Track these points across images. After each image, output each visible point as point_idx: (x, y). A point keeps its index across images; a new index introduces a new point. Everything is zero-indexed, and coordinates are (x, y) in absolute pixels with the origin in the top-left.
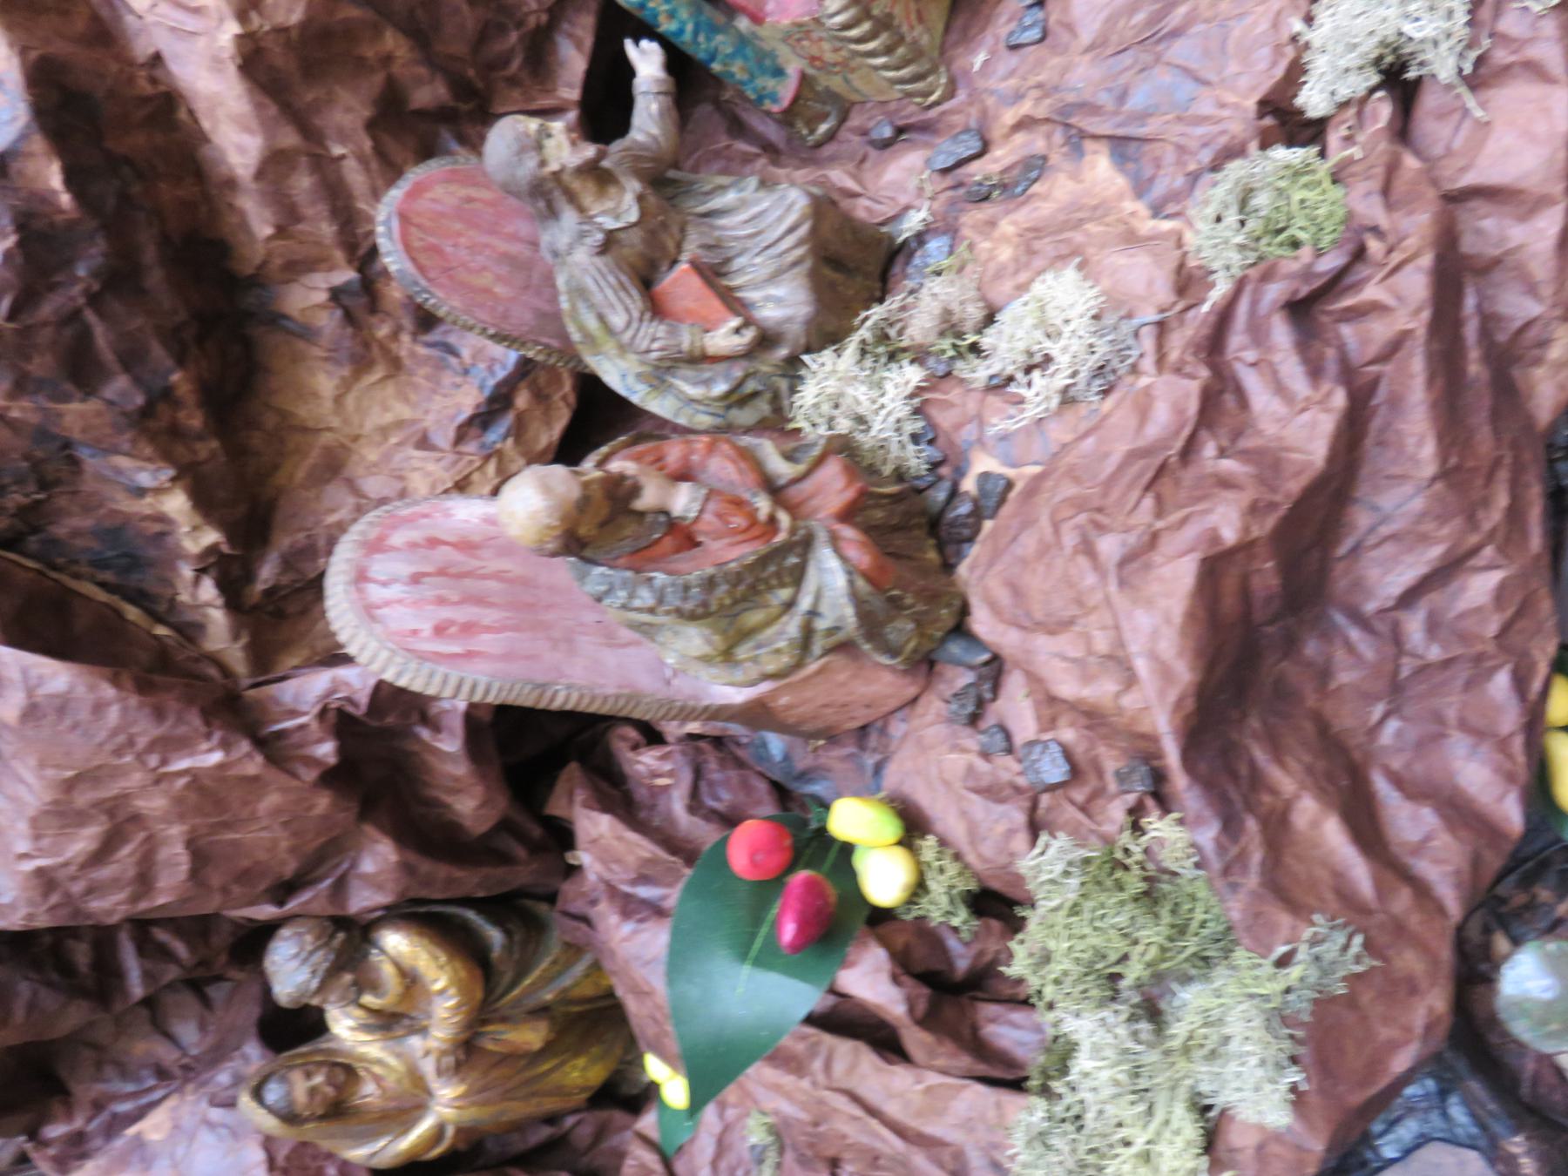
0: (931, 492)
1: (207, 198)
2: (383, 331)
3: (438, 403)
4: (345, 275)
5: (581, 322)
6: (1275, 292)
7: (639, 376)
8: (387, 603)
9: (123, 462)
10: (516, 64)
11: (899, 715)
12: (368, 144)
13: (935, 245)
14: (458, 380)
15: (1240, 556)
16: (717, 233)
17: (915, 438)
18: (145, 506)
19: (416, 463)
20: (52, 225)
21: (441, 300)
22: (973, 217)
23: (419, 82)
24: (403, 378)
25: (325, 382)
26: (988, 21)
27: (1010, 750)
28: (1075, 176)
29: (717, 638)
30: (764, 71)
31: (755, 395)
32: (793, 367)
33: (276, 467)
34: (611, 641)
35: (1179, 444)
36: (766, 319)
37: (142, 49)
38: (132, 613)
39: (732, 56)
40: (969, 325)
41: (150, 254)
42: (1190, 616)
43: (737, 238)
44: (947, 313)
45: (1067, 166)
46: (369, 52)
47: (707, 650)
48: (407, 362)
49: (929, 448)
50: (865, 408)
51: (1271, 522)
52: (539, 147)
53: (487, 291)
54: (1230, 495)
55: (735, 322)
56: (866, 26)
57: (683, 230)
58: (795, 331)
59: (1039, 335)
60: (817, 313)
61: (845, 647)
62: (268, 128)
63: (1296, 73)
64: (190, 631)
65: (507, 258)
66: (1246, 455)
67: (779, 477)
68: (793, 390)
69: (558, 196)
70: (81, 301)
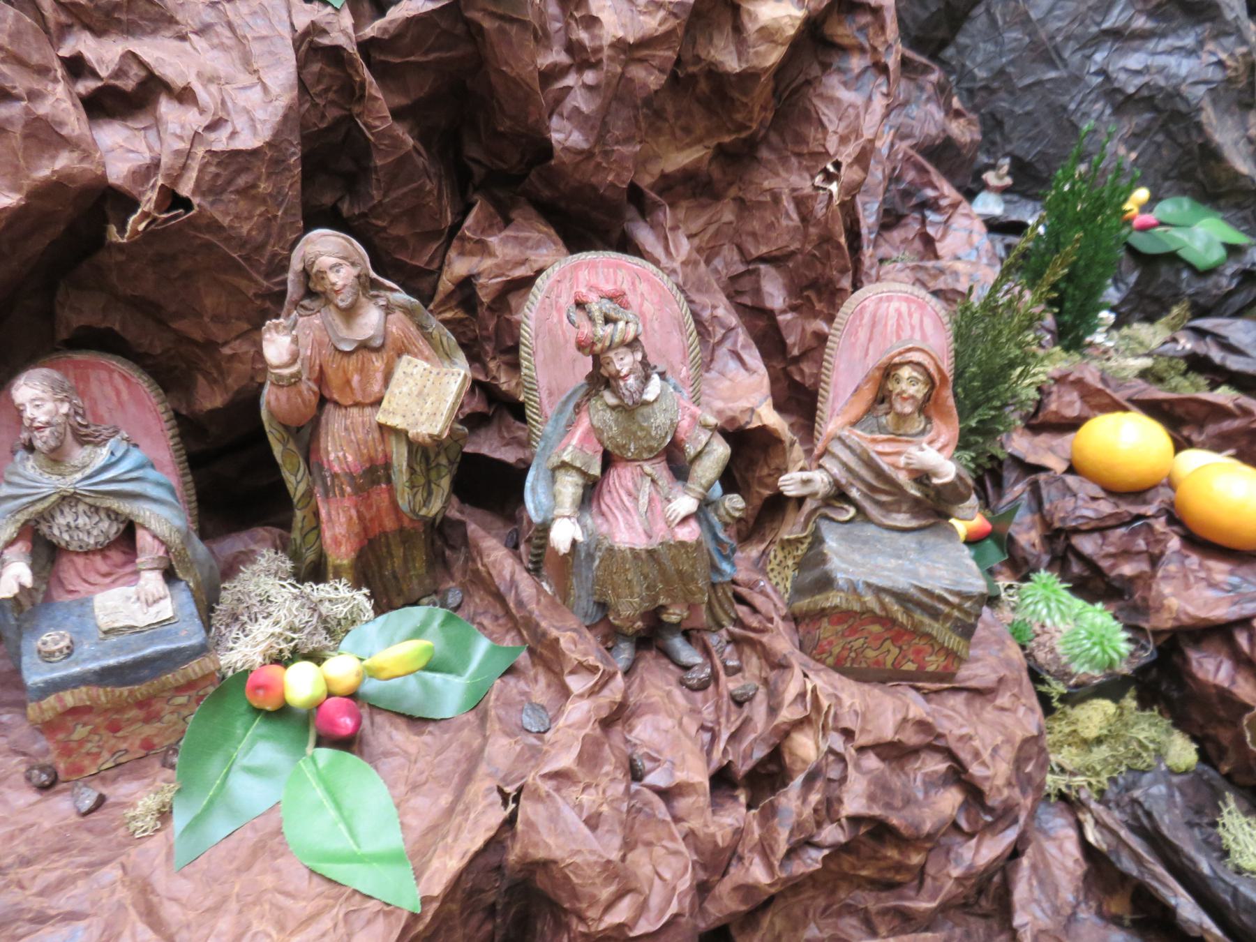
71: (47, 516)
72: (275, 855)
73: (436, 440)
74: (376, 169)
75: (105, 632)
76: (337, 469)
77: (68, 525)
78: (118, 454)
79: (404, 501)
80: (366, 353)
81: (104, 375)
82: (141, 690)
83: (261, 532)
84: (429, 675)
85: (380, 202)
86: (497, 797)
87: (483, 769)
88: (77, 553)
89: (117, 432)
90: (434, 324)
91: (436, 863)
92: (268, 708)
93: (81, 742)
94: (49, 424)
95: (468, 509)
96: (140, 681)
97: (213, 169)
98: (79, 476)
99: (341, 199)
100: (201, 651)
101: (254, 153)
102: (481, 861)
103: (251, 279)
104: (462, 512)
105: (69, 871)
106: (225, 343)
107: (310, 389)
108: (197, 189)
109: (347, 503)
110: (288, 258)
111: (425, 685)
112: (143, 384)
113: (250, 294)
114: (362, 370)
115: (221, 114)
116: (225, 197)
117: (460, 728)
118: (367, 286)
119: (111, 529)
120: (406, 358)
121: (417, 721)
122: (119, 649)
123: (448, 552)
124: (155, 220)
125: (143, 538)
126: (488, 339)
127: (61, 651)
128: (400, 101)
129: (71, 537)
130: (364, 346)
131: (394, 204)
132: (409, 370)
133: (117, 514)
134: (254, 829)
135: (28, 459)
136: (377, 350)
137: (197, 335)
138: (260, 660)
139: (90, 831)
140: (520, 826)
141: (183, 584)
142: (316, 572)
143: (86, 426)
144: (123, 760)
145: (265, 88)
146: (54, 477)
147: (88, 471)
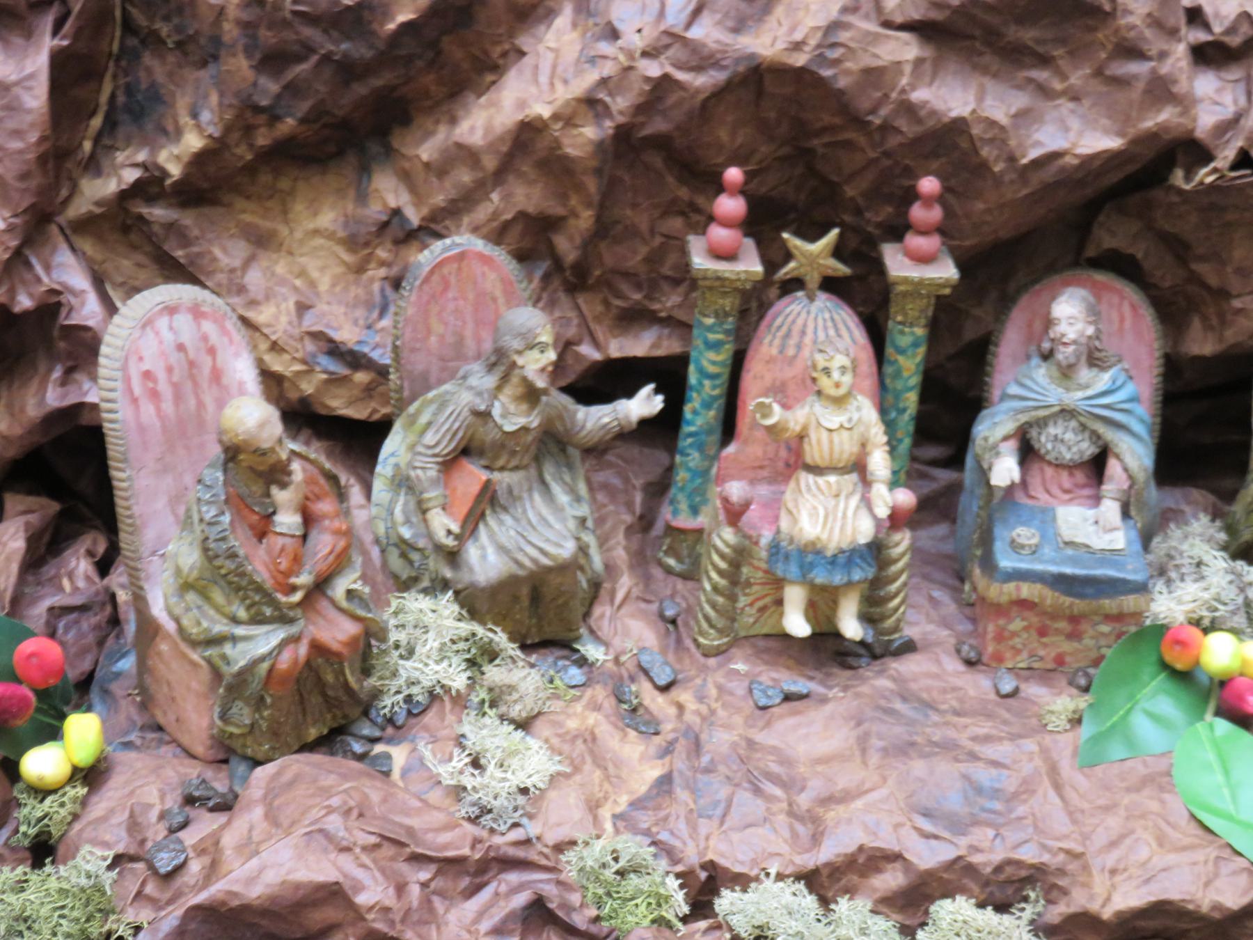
0: (368, 723)
1: (438, 104)
2: (382, 253)
3: (340, 310)
4: (414, 216)
5: (423, 410)
6: (550, 890)
7: (397, 466)
8: (157, 333)
9: (214, 98)
11: (178, 750)
12: (508, 216)
13: (576, 674)
14: (361, 322)
15: (352, 914)
16: (525, 495)
17: (408, 699)
18: (185, 120)
19: (283, 306)
20: (370, 22)
21: (409, 300)
22: (600, 693)
23: (571, 239)
24: (351, 277)
25: (328, 218)
26: (772, 664)
27: (172, 831)
28: (642, 758)
29: (195, 574)
30: (690, 497)
31: (411, 562)
33: (248, 198)
34: (175, 500)
35: (420, 850)
36: (467, 552)
37: (524, 41)
38: (97, 122)
39: (689, 469)
40: (503, 709)
41: (377, 82)
42: (298, 886)
43: (525, 511)
44: (511, 688)
45: (652, 750)
46: (574, 201)
47: (186, 569)
48: (365, 277)
49: (404, 713)
50: (420, 650)
51: (380, 926)
52: (531, 347)
53: (429, 332)
54: (391, 891)
55: (455, 528)
56: (723, 565)
57: (516, 468)
58: (464, 578)
59: (499, 754)
60: (483, 590)
61: (217, 675)
62: (491, 147)
63: (742, 881)
64: (93, 166)
65: (460, 342)
66: (427, 903)
67: (333, 589)
68: (425, 591)
69: (501, 369)
70: (323, 52)
71: (1042, 423)
72: (1162, 789)
75: (1066, 543)
77: (1056, 436)
78: (1119, 383)
81: (1116, 299)
82: (1079, 605)
83: (1196, 494)
88: (1050, 463)
89: (1120, 361)
92: (1179, 666)
93: (1014, 634)
94: (1075, 342)
98: (1080, 394)
105: (994, 732)
106: (1239, 296)
112: (1148, 315)
119: (1088, 449)
122: (1074, 561)
125: (1113, 467)
127: (1030, 546)
129: (1054, 448)
133: (1099, 437)
134: (1145, 764)
135: (1039, 366)
137: (1213, 281)
138: (1181, 618)
139: (1008, 710)
144: (1036, 665)
146: (1060, 390)
147: (1090, 392)
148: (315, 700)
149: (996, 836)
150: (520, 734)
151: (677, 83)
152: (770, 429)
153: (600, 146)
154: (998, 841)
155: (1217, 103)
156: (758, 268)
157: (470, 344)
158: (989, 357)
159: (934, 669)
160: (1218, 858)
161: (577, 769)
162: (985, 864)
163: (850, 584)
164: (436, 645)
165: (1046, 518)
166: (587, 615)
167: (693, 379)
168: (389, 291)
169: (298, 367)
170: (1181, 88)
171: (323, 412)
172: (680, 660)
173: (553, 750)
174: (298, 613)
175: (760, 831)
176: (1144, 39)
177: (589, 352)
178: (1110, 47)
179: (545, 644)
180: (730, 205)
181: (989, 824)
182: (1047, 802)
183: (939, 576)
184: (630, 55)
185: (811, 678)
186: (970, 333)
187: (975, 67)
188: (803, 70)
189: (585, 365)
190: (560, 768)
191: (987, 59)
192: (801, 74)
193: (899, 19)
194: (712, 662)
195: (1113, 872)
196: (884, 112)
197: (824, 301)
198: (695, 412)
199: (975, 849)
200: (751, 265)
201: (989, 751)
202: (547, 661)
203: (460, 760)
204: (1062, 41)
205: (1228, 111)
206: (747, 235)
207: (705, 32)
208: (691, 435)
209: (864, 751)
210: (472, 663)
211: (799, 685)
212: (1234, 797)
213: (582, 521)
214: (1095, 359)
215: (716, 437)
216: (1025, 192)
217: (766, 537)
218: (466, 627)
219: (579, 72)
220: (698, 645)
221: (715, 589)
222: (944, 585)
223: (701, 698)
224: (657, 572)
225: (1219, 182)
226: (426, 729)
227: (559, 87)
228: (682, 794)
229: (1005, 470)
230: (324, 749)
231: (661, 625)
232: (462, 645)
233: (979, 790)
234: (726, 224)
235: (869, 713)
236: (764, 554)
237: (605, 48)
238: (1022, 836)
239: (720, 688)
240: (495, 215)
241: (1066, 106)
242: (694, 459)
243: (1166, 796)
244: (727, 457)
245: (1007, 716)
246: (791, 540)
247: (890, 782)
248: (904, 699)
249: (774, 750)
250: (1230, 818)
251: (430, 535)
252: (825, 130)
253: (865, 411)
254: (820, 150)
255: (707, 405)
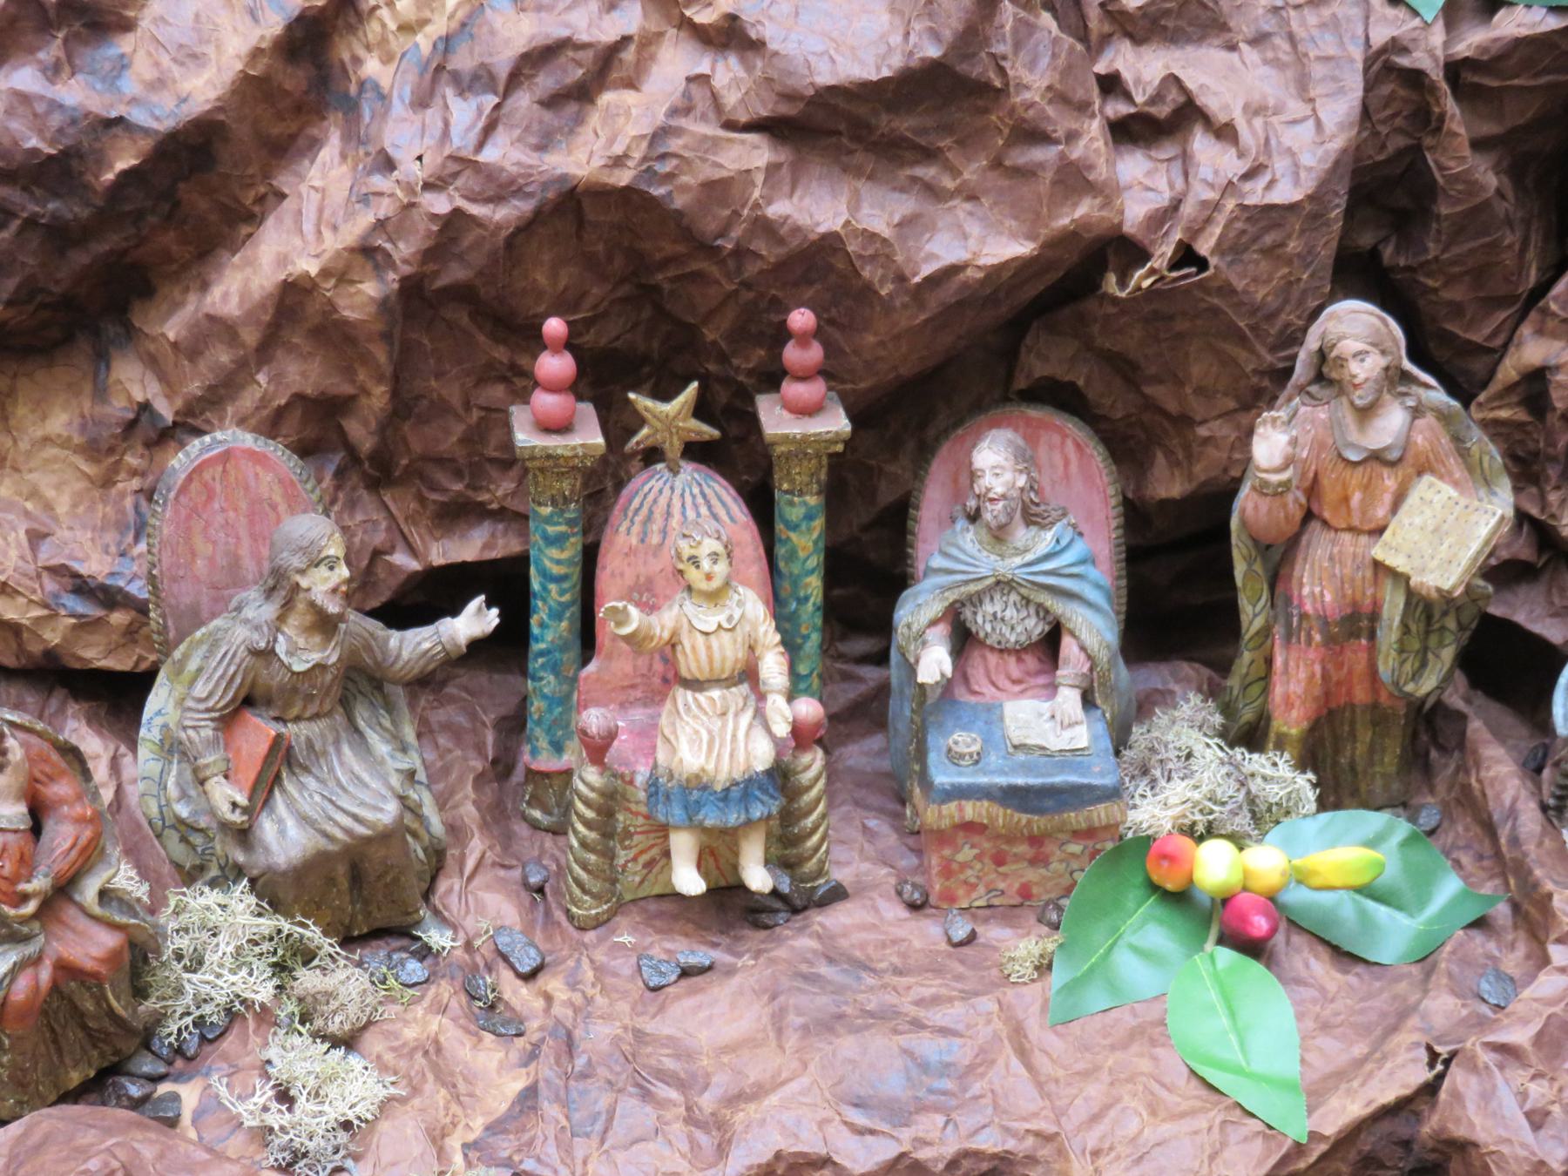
0: (150, 1057)
1: (185, 267)
2: (132, 460)
4: (166, 411)
7: (165, 726)
10: (435, 496)
13: (415, 969)
14: (113, 549)
16: (331, 749)
17: (200, 1022)
19: (12, 537)
20: (81, 173)
21: (164, 520)
22: (444, 990)
23: (365, 423)
24: (97, 494)
25: (60, 422)
26: (664, 932)
28: (501, 1067)
30: (548, 731)
31: (194, 847)
32: (231, 874)
36: (261, 827)
37: (283, 181)
39: (544, 697)
40: (319, 1023)
41: (101, 247)
43: (331, 770)
44: (329, 995)
45: (514, 1056)
46: (362, 375)
48: (114, 491)
49: (196, 1039)
50: (211, 958)
53: (193, 554)
55: (242, 800)
56: (590, 814)
57: (316, 716)
58: (258, 862)
59: (312, 1083)
60: (284, 874)
62: (250, 316)
65: (235, 564)
67: (81, 893)
68: (213, 884)
70: (25, 215)
71: (976, 600)
72: (1153, 1042)
73: (1446, 597)
74: (1438, 216)
75: (1015, 747)
76: (1309, 608)
77: (995, 615)
78: (1064, 543)
79: (1386, 667)
80: (1376, 466)
81: (1056, 439)
82: (1039, 822)
83: (1186, 668)
84: (1371, 905)
85: (1436, 259)
86: (1424, 1056)
87: (1414, 1021)
88: (992, 649)
89: (1064, 515)
90: (1478, 440)
91: (1334, 1102)
92: (1170, 887)
93: (964, 866)
94: (1004, 497)
95: (1480, 699)
96: (1041, 811)
97: (1239, 225)
98: (1018, 561)
99: (1385, 240)
100: (1113, 794)
101: (1292, 208)
102: (1385, 1126)
103: (1253, 351)
104: (1468, 701)
105: (944, 991)
106: (1204, 422)
107: (1296, 500)
108: (1218, 249)
109: (1312, 654)
110: (1305, 330)
111: (1363, 916)
112: (1097, 455)
113: (1249, 368)
114: (1366, 488)
115: (1262, 159)
116: (1246, 257)
117: (1398, 979)
118: (1396, 379)
119: (1035, 628)
120: (1428, 478)
121: (1344, 957)
122: (1027, 768)
123: (1434, 754)
124: (1162, 278)
125: (1068, 647)
126: (1553, 459)
127: (971, 755)
128: (1488, 128)
129: (993, 629)
130: (1376, 457)
131: (1454, 262)
132: (1429, 495)
133: (1047, 612)
134: (1134, 1013)
135: (968, 530)
136: (1392, 464)
137: (1172, 406)
138: (1169, 826)
139: (962, 962)
140: (1443, 1095)
141: (1099, 712)
142: (1252, 736)
143: (1037, 505)
144: (996, 902)
145: (1319, 124)
146: (993, 557)
147: (1029, 557)
148: (73, 1035)
149: (947, 1123)
150: (339, 1053)
151: (472, 218)
152: (628, 639)
153: (383, 304)
154: (950, 1127)
155: (1149, 189)
156: (600, 440)
157: (248, 564)
158: (910, 523)
159: (870, 918)
160: (1224, 1122)
161: (416, 1090)
162: (936, 1160)
163: (749, 823)
164: (230, 949)
165: (992, 714)
166: (427, 895)
167: (535, 585)
168: (143, 503)
169: (38, 612)
170: (1100, 173)
171: (77, 666)
172: (549, 938)
173: (383, 1068)
174: (36, 926)
175: (651, 1146)
176: (1048, 118)
177: (404, 561)
178: (1006, 131)
179: (379, 933)
180: (555, 365)
181: (936, 1109)
182: (1009, 1073)
183: (875, 800)
184: (409, 189)
185: (715, 945)
186: (886, 495)
187: (845, 169)
188: (628, 191)
189: (402, 577)
190: (393, 1090)
191: (859, 157)
192: (628, 196)
193: (743, 118)
194: (590, 936)
195: (1096, 1154)
196: (736, 233)
197: (690, 472)
198: (542, 625)
199: (921, 1142)
200: (589, 437)
201: (937, 1017)
202: (377, 955)
203: (263, 1095)
204: (947, 129)
205: (1163, 199)
206: (580, 398)
207: (501, 153)
208: (542, 654)
209: (779, 1032)
210: (280, 968)
211: (700, 955)
212: (1242, 1044)
213: (410, 775)
214: (1032, 516)
215: (574, 653)
216: (923, 317)
217: (642, 776)
218: (267, 924)
219: (350, 215)
220: (570, 917)
221: (584, 844)
222: (881, 811)
223: (573, 985)
224: (521, 829)
225: (1158, 285)
226: (225, 1057)
227: (327, 234)
228: (551, 1110)
229: (935, 662)
230: (93, 1097)
231: (524, 895)
232: (266, 946)
233: (924, 1067)
234: (552, 389)
235: (785, 982)
236: (642, 795)
237: (379, 182)
238: (979, 1119)
239: (599, 970)
240: (264, 401)
241: (962, 208)
242: (549, 683)
243: (1159, 1051)
244: (587, 678)
245: (961, 969)
246: (671, 776)
247: (812, 1067)
248: (831, 960)
249: (671, 1041)
250: (1238, 1071)
251: (212, 812)
252: (666, 263)
253: (751, 606)
254: (666, 286)
255: (557, 616)
